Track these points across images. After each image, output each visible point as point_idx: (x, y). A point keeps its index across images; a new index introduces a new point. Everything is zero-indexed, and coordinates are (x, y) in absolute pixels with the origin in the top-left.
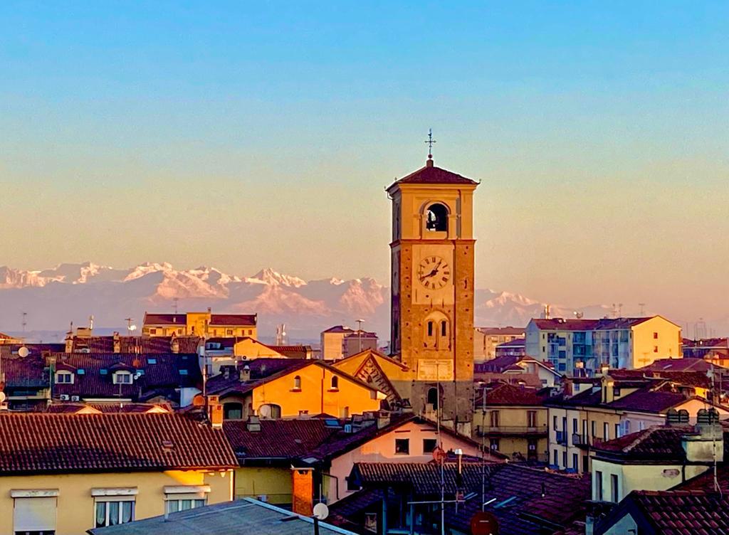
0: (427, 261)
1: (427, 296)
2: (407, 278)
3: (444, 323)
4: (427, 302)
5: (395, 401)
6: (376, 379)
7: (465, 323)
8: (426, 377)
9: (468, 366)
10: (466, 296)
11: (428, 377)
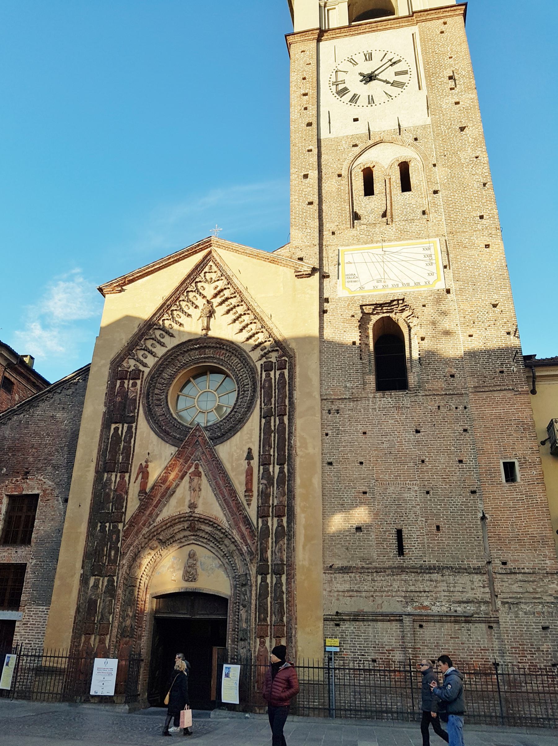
1: (356, 120)
3: (404, 168)
6: (224, 308)
7: (461, 155)
8: (362, 288)
9: (487, 246)
10: (457, 103)
11: (367, 287)
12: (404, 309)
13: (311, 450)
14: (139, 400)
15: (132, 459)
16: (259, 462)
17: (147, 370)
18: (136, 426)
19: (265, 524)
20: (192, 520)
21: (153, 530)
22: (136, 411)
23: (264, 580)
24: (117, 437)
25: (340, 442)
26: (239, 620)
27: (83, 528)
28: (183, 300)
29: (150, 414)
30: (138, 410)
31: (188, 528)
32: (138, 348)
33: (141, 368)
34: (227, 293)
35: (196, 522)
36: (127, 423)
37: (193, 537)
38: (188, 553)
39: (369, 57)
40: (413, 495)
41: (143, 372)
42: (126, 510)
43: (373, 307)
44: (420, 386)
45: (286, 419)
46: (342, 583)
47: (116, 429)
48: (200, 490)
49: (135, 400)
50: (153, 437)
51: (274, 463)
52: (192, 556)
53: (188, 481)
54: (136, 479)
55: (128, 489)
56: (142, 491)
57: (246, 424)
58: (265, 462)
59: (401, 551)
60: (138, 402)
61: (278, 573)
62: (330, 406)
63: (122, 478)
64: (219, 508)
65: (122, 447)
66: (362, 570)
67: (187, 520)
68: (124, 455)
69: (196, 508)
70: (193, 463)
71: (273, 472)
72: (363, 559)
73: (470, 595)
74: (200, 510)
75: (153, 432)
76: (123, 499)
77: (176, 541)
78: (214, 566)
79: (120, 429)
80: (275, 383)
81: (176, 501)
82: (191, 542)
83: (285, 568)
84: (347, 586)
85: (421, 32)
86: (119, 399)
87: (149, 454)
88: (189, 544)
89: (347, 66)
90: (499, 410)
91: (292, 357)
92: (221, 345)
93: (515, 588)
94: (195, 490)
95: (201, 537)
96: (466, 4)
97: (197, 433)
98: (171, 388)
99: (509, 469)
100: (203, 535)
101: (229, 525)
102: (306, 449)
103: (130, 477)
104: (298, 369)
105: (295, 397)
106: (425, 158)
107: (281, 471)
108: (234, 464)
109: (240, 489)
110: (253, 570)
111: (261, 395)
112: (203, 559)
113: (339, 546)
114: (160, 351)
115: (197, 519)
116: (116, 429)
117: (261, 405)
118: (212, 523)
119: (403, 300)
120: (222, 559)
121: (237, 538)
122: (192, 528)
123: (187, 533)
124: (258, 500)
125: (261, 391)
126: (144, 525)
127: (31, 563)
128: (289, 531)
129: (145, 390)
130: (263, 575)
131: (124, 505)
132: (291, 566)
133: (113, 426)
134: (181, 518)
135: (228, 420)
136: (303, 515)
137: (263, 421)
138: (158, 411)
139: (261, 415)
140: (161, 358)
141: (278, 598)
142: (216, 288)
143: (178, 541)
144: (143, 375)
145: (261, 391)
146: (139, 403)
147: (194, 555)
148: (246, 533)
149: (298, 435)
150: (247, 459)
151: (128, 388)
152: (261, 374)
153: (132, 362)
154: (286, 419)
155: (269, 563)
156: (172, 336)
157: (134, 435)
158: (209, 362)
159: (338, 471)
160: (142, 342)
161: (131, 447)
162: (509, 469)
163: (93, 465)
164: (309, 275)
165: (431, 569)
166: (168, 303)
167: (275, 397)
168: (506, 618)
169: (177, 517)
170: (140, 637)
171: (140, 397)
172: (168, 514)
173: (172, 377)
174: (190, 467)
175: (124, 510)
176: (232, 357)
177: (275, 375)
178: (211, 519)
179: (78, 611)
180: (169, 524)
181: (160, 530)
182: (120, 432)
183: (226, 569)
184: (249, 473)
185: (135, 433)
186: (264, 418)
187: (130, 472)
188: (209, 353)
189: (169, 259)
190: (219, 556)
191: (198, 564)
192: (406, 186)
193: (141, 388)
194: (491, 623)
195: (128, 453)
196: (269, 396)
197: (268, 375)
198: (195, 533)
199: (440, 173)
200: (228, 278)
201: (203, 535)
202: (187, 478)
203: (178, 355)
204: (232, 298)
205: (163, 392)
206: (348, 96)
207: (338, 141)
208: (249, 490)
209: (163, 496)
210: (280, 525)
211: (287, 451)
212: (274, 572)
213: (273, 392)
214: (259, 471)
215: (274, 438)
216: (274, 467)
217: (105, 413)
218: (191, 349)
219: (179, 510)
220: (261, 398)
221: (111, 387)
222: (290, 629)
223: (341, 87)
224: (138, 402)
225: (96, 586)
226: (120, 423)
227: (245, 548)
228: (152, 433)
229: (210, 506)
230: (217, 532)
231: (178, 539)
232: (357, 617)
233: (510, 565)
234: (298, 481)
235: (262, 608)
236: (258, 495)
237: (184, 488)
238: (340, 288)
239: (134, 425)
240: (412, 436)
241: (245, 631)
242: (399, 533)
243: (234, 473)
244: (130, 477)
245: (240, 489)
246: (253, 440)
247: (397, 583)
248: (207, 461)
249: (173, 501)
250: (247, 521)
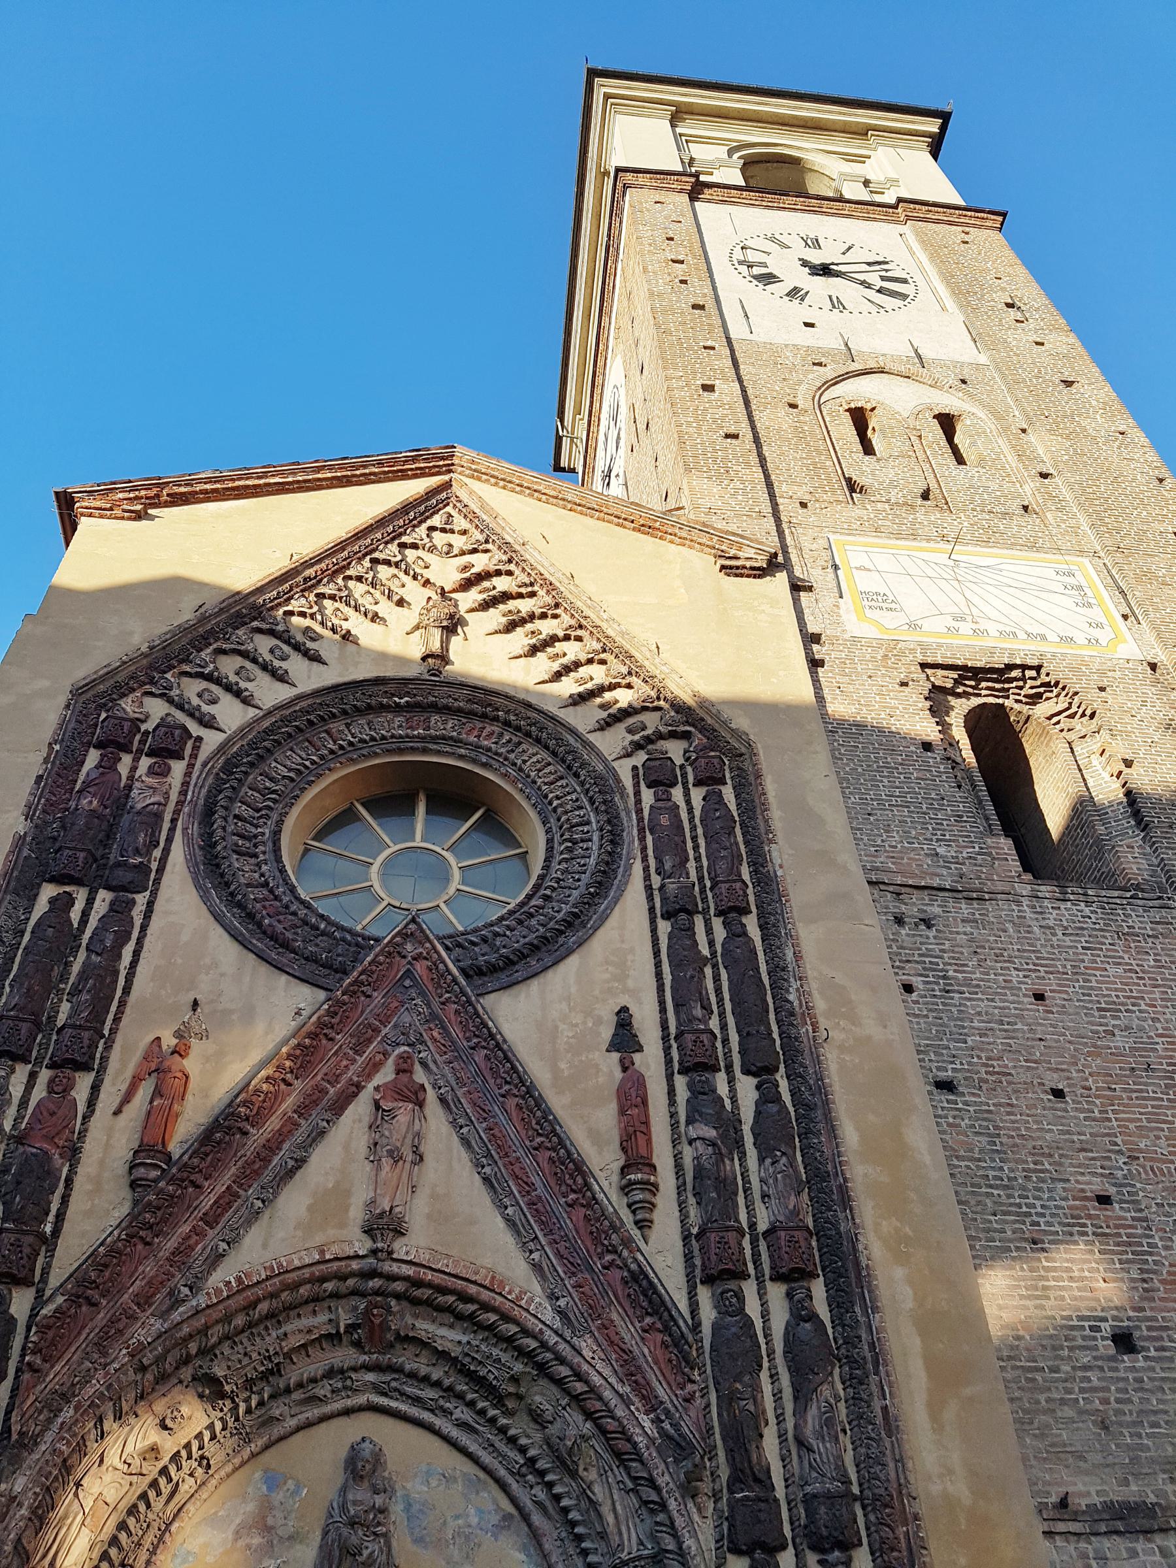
12: (1039, 696)
13: (871, 1028)
14: (174, 821)
15: (117, 1020)
16: (669, 1061)
17: (212, 740)
18: (150, 904)
19: (730, 1307)
20: (377, 1292)
21: (186, 1330)
22: (157, 853)
24: (59, 934)
25: (962, 1016)
28: (359, 579)
29: (211, 869)
30: (166, 851)
31: (351, 1328)
32: (187, 668)
35: (393, 1303)
36: (108, 888)
37: (371, 1377)
38: (343, 1453)
41: (199, 739)
42: (56, 1232)
43: (954, 675)
45: (751, 924)
47: (62, 904)
48: (420, 1158)
49: (159, 816)
50: (224, 950)
51: (729, 1068)
53: (366, 1120)
54: (127, 1098)
55: (83, 1134)
56: (149, 1150)
57: (600, 933)
58: (695, 1063)
60: (166, 825)
63: (60, 1090)
64: (507, 1240)
65: (76, 968)
67: (354, 1293)
68: (85, 996)
69: (399, 1233)
70: (386, 1054)
71: (734, 1099)
74: (415, 1245)
75: (220, 930)
76: (50, 1174)
77: (288, 1391)
78: (474, 1520)
79: (79, 906)
80: (691, 819)
81: (308, 1201)
82: (361, 1399)
86: (89, 803)
87: (195, 1004)
88: (347, 1412)
92: (486, 704)
95: (412, 1375)
96: (1004, 215)
97: (409, 947)
98: (295, 812)
100: (421, 1365)
101: (562, 1313)
102: (854, 1020)
103: (95, 1088)
105: (777, 861)
108: (563, 1065)
109: (603, 1161)
111: (644, 849)
112: (416, 1488)
113: (1068, 1412)
114: (270, 694)
115: (399, 1286)
116: (62, 904)
117: (647, 877)
118: (471, 1307)
119: (1038, 668)
120: (515, 1486)
122: (369, 1334)
123: (344, 1356)
124: (682, 1205)
125: (642, 839)
126: (143, 1300)
128: (851, 1341)
129: (198, 795)
130: (758, 1555)
131: (54, 1208)
134: (323, 1279)
135: (520, 922)
136: (899, 1273)
137: (664, 927)
138: (243, 870)
139: (652, 910)
140: (269, 713)
142: (465, 568)
143: (297, 1395)
144: (196, 748)
145: (642, 839)
146: (172, 830)
147: (377, 1459)
148: (644, 1351)
149: (810, 973)
150: (614, 1046)
151: (131, 778)
152: (637, 793)
154: (751, 924)
155: (780, 1492)
156: (316, 658)
157: (135, 934)
158: (438, 753)
159: (984, 1114)
160: (206, 654)
161: (116, 973)
164: (760, 573)
166: (310, 572)
167: (698, 859)
169: (306, 1273)
171: (177, 812)
172: (268, 1256)
173: (302, 778)
174: (374, 1067)
175: (48, 1229)
176: (524, 746)
178: (473, 1290)
180: (264, 1307)
181: (216, 1333)
182: (75, 915)
183: (535, 1535)
185: (144, 928)
186: (667, 916)
187: (102, 1069)
189: (319, 469)
190: (502, 1472)
191: (397, 1510)
193: (185, 784)
195: (104, 993)
198: (384, 1359)
201: (421, 1365)
202: (360, 1110)
203: (334, 716)
204: (520, 596)
205: (267, 817)
209: (248, 1175)
210: (801, 1313)
211: (775, 1028)
213: (690, 845)
214: (671, 1092)
215: (716, 984)
216: (731, 1081)
217: (19, 842)
218: (383, 708)
219: (319, 1239)
220: (645, 859)
224: (166, 825)
226: (79, 882)
227: (647, 1424)
228: (218, 935)
230: (495, 1352)
231: (300, 1385)
234: (850, 1135)
236: (681, 1189)
237: (346, 1147)
239: (141, 899)
243: (566, 1099)
244: (95, 1088)
245: (603, 1161)
246: (630, 983)
249: (294, 1202)
250: (643, 1291)
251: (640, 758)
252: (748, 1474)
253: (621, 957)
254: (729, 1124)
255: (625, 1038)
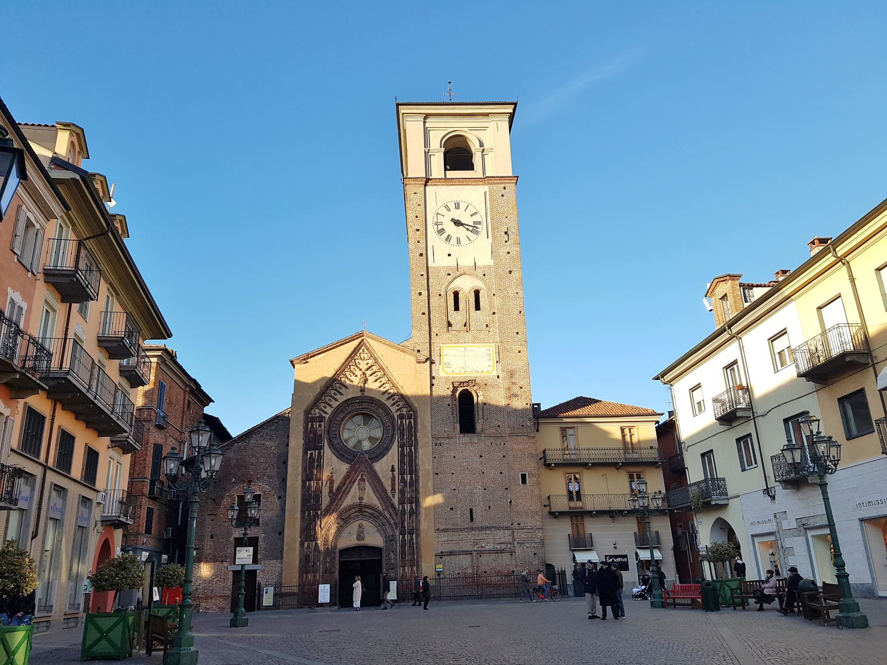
0: (446, 207)
1: (449, 255)
2: (418, 230)
3: (477, 293)
4: (451, 262)
5: (404, 411)
9: (519, 352)
11: (457, 371)
13: (427, 467)
17: (327, 416)
19: (403, 507)
23: (403, 537)
26: (390, 559)
27: (298, 515)
29: (331, 444)
33: (323, 414)
34: (375, 368)
39: (457, 206)
40: (478, 491)
44: (482, 431)
46: (444, 537)
52: (360, 526)
56: (331, 491)
58: (402, 473)
59: (472, 520)
61: (411, 534)
62: (437, 441)
66: (453, 530)
72: (453, 524)
73: (503, 540)
83: (415, 531)
84: (446, 539)
85: (490, 192)
86: (311, 435)
89: (443, 211)
90: (521, 446)
91: (415, 412)
93: (523, 536)
94: (362, 489)
99: (524, 477)
104: (419, 420)
106: (489, 289)
107: (411, 478)
109: (389, 489)
110: (397, 533)
114: (335, 404)
116: (311, 454)
121: (388, 516)
122: (360, 511)
127: (261, 536)
132: (418, 529)
133: (309, 452)
138: (335, 441)
141: (411, 546)
153: (317, 411)
162: (524, 477)
163: (300, 477)
165: (486, 528)
168: (518, 550)
170: (334, 573)
177: (406, 422)
179: (300, 561)
184: (393, 479)
188: (365, 405)
192: (478, 307)
194: (512, 552)
196: (402, 435)
197: (402, 422)
199: (497, 301)
200: (375, 359)
202: (357, 482)
206: (444, 236)
207: (438, 269)
208: (393, 489)
210: (412, 508)
212: (409, 533)
215: (406, 459)
221: (306, 427)
222: (418, 562)
223: (440, 227)
225: (308, 547)
229: (371, 498)
232: (451, 553)
233: (522, 525)
235: (403, 552)
238: (441, 371)
240: (478, 459)
241: (394, 564)
242: (471, 510)
245: (389, 489)
247: (470, 536)
248: (368, 472)
249: (349, 496)
250: (393, 505)
251: (399, 412)
252: (403, 527)
253: (392, 457)
254: (405, 483)
255: (393, 470)
